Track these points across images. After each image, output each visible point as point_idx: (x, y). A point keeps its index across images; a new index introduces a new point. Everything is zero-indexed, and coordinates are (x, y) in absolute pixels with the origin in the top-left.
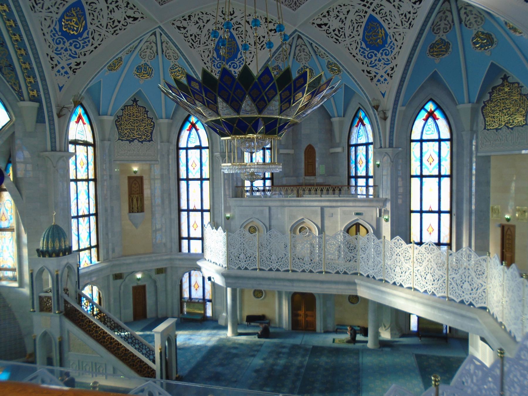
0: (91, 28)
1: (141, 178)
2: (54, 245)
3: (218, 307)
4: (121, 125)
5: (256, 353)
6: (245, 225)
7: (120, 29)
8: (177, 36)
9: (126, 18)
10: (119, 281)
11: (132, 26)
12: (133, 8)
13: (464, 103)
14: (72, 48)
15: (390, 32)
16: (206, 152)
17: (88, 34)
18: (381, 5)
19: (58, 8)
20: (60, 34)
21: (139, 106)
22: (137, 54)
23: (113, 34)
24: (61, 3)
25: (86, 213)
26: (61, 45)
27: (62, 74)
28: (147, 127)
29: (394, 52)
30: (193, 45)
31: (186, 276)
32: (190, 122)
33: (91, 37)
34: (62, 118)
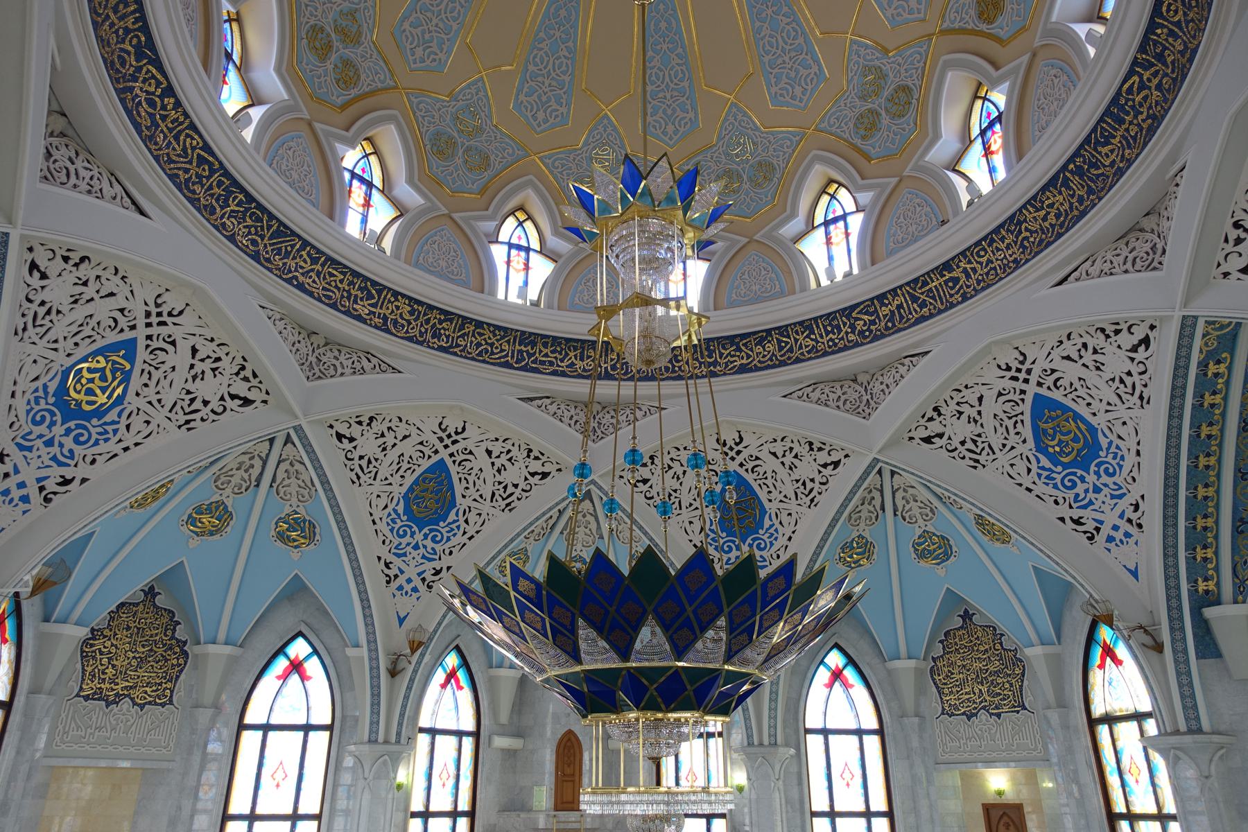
0: (132, 402)
7: (202, 420)
8: (330, 454)
9: (227, 397)
11: (236, 417)
12: (251, 378)
13: (899, 659)
14: (69, 442)
15: (771, 508)
16: (319, 741)
17: (119, 415)
18: (757, 458)
19: (76, 344)
20: (52, 400)
23: (179, 427)
24: (89, 337)
26: (42, 429)
27: (11, 501)
29: (777, 545)
30: (359, 478)
33: (124, 421)
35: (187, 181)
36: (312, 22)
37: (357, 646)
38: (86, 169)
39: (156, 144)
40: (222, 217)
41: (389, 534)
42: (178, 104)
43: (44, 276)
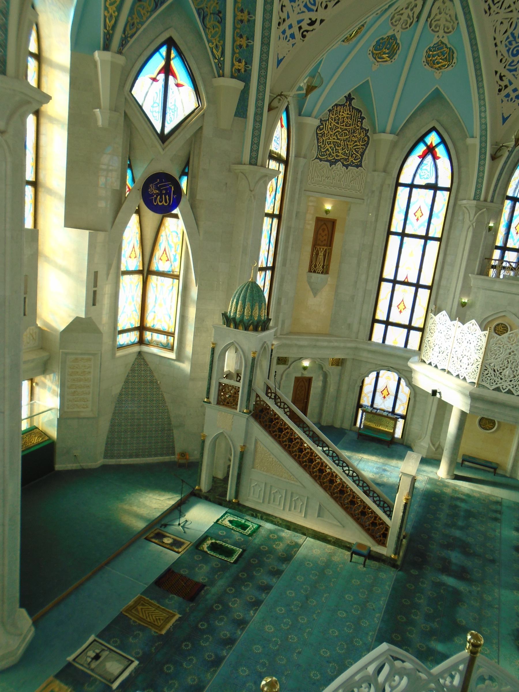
1: (333, 222)
2: (252, 312)
3: (415, 428)
4: (323, 135)
5: (498, 516)
6: (490, 319)
10: (282, 367)
16: (443, 197)
21: (353, 108)
22: (389, 16)
25: (264, 266)
28: (358, 143)
31: (373, 375)
32: (426, 144)
34: (272, 112)
37: (473, 137)
41: (505, 54)
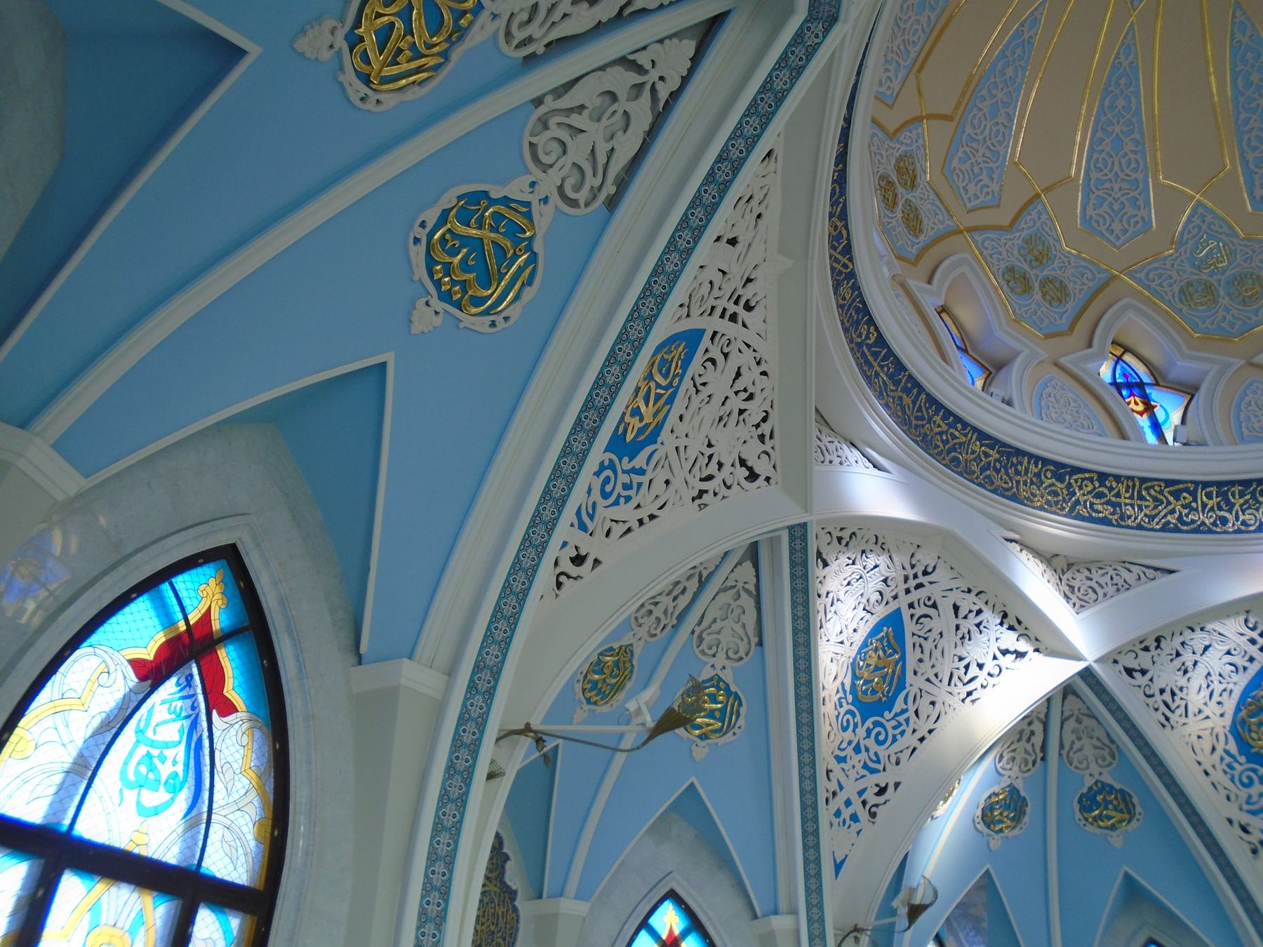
20: (1242, 759)
35: (1180, 519)
36: (1176, 289)
38: (1103, 575)
39: (1129, 517)
40: (1237, 519)
42: (1118, 478)
43: (1144, 672)
